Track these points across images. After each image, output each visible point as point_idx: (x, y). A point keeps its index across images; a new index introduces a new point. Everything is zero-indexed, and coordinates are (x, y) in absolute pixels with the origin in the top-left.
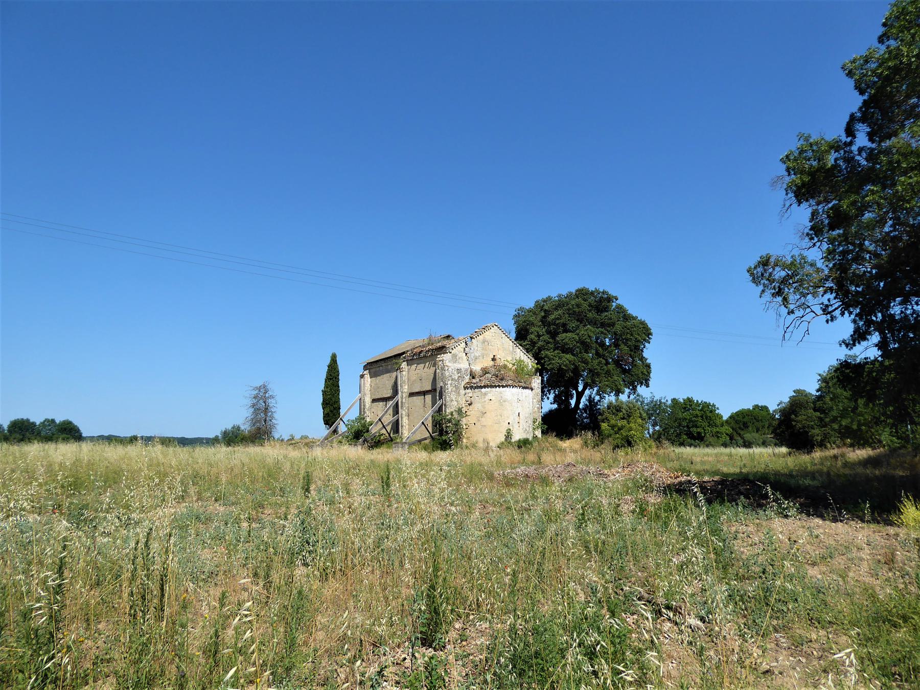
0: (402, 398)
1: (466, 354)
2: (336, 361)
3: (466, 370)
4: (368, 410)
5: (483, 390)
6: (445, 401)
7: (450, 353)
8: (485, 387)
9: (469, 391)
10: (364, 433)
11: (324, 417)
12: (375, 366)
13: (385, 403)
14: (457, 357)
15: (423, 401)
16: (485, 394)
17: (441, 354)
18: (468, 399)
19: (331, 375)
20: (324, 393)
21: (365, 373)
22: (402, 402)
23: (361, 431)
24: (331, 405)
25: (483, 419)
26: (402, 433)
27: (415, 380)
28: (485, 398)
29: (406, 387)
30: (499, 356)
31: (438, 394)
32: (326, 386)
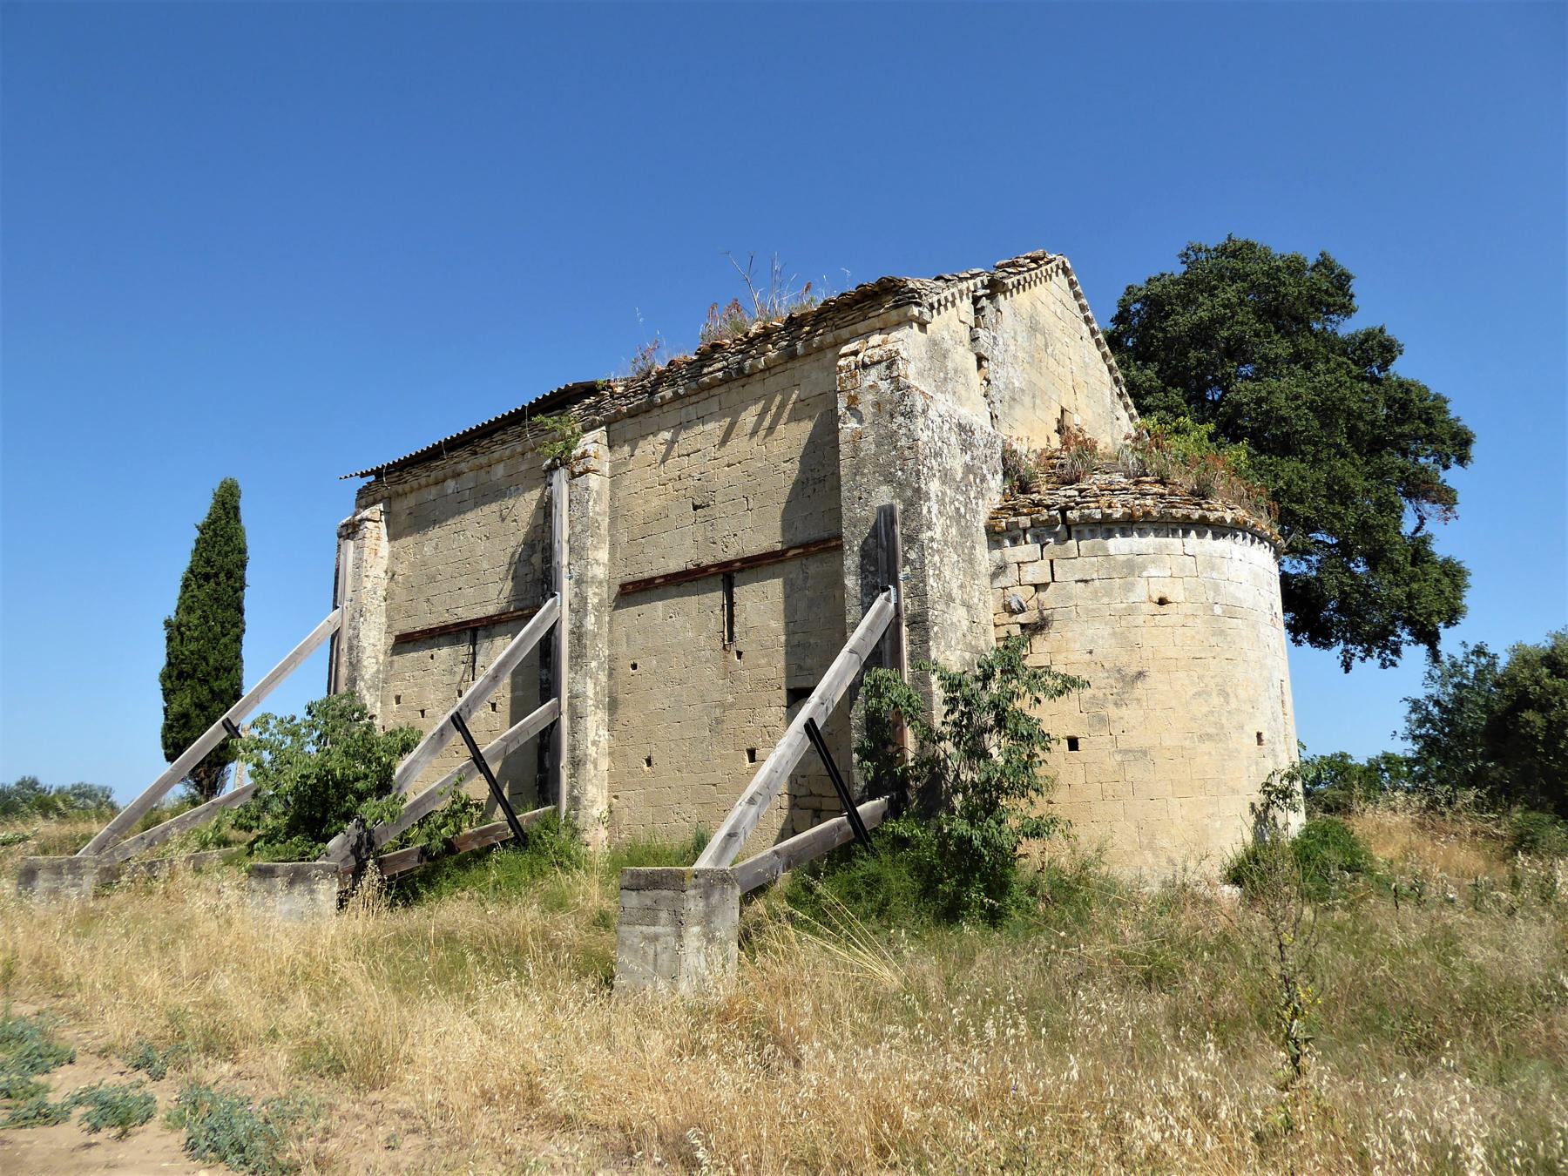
0: (579, 610)
1: (980, 359)
2: (236, 509)
4: (373, 687)
5: (1118, 545)
6: (919, 594)
7: (923, 326)
8: (1130, 525)
9: (1027, 550)
10: (361, 797)
11: (168, 728)
12: (422, 476)
13: (464, 649)
15: (719, 616)
16: (1132, 568)
17: (866, 335)
18: (1022, 594)
19: (208, 562)
20: (175, 631)
21: (366, 513)
22: (578, 634)
23: (343, 786)
24: (203, 681)
25: (1129, 715)
26: (575, 801)
27: (662, 515)
28: (1129, 588)
29: (603, 555)
31: (851, 561)
32: (186, 606)
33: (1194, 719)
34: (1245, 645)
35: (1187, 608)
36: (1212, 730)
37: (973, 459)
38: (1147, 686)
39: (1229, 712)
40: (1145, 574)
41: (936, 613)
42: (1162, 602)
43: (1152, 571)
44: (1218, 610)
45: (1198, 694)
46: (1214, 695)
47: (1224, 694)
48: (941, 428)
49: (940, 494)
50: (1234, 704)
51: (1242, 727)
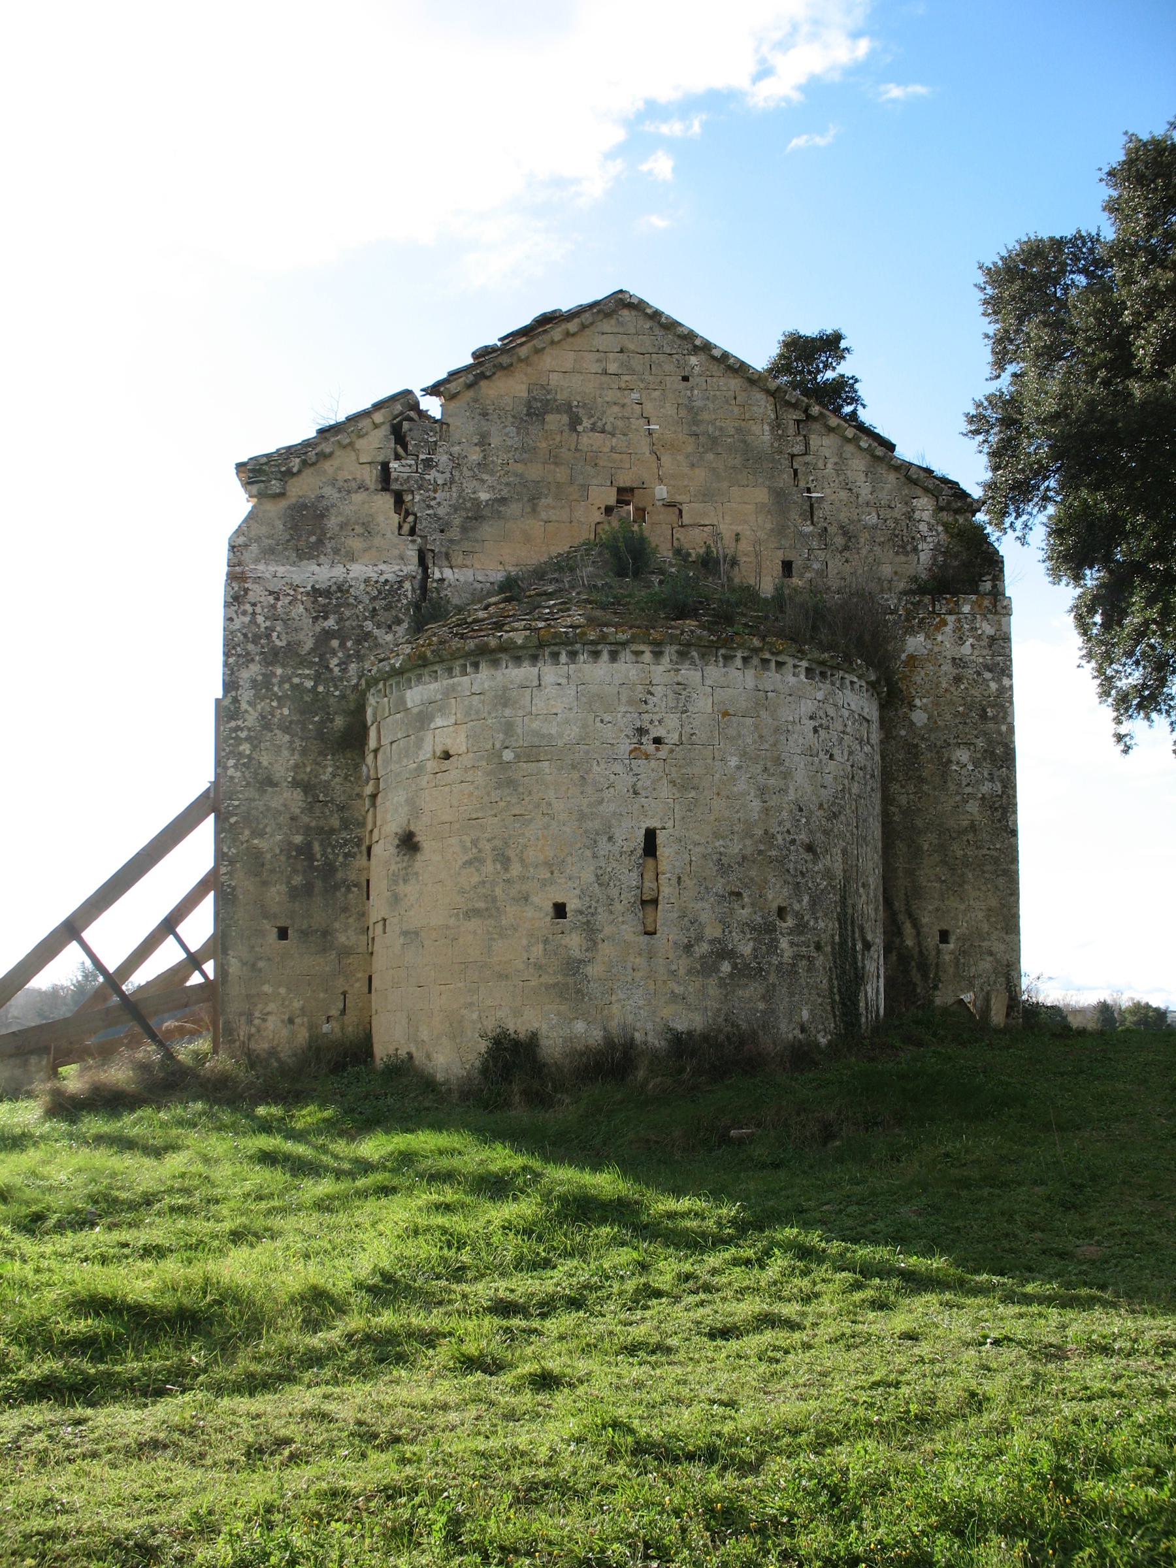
3: (388, 592)
14: (332, 522)
25: (409, 890)
30: (661, 492)
33: (462, 892)
34: (551, 795)
35: (467, 760)
36: (481, 905)
37: (340, 621)
38: (423, 858)
39: (507, 881)
40: (432, 726)
41: (237, 803)
42: (447, 756)
43: (439, 722)
44: (508, 755)
45: (469, 863)
46: (489, 862)
47: (505, 862)
48: (274, 607)
49: (260, 678)
50: (516, 870)
51: (526, 898)
